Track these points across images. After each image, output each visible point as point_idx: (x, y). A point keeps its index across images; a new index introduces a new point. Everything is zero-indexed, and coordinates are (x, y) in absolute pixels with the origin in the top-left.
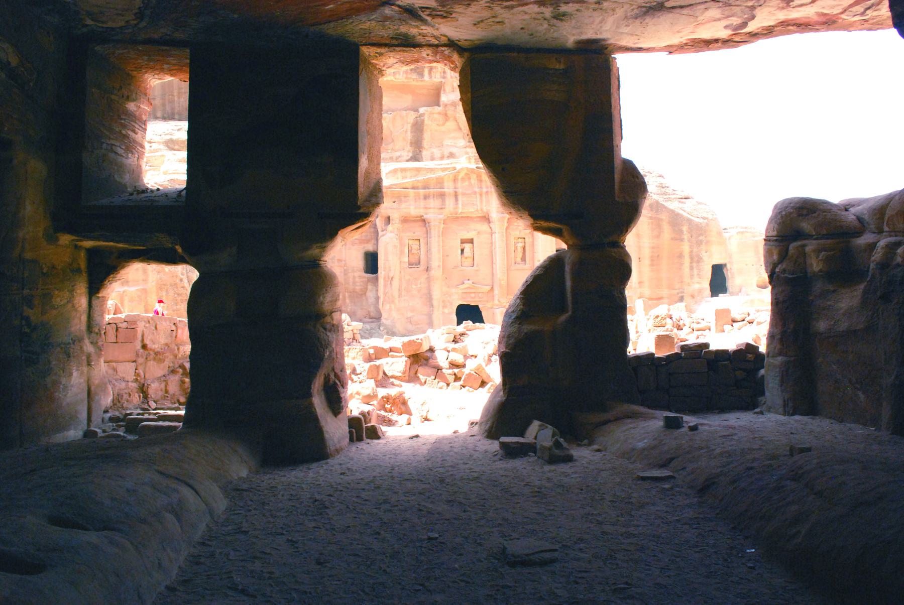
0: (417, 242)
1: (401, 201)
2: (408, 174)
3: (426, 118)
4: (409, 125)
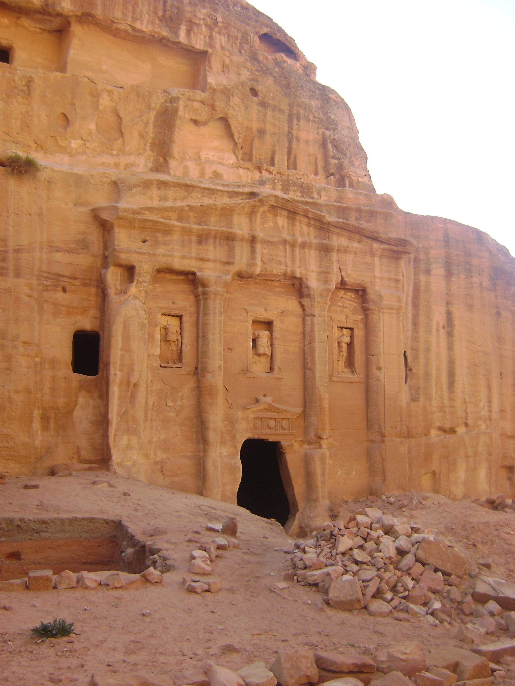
0: (174, 323)
1: (156, 243)
2: (171, 193)
3: (181, 104)
4: (152, 115)
